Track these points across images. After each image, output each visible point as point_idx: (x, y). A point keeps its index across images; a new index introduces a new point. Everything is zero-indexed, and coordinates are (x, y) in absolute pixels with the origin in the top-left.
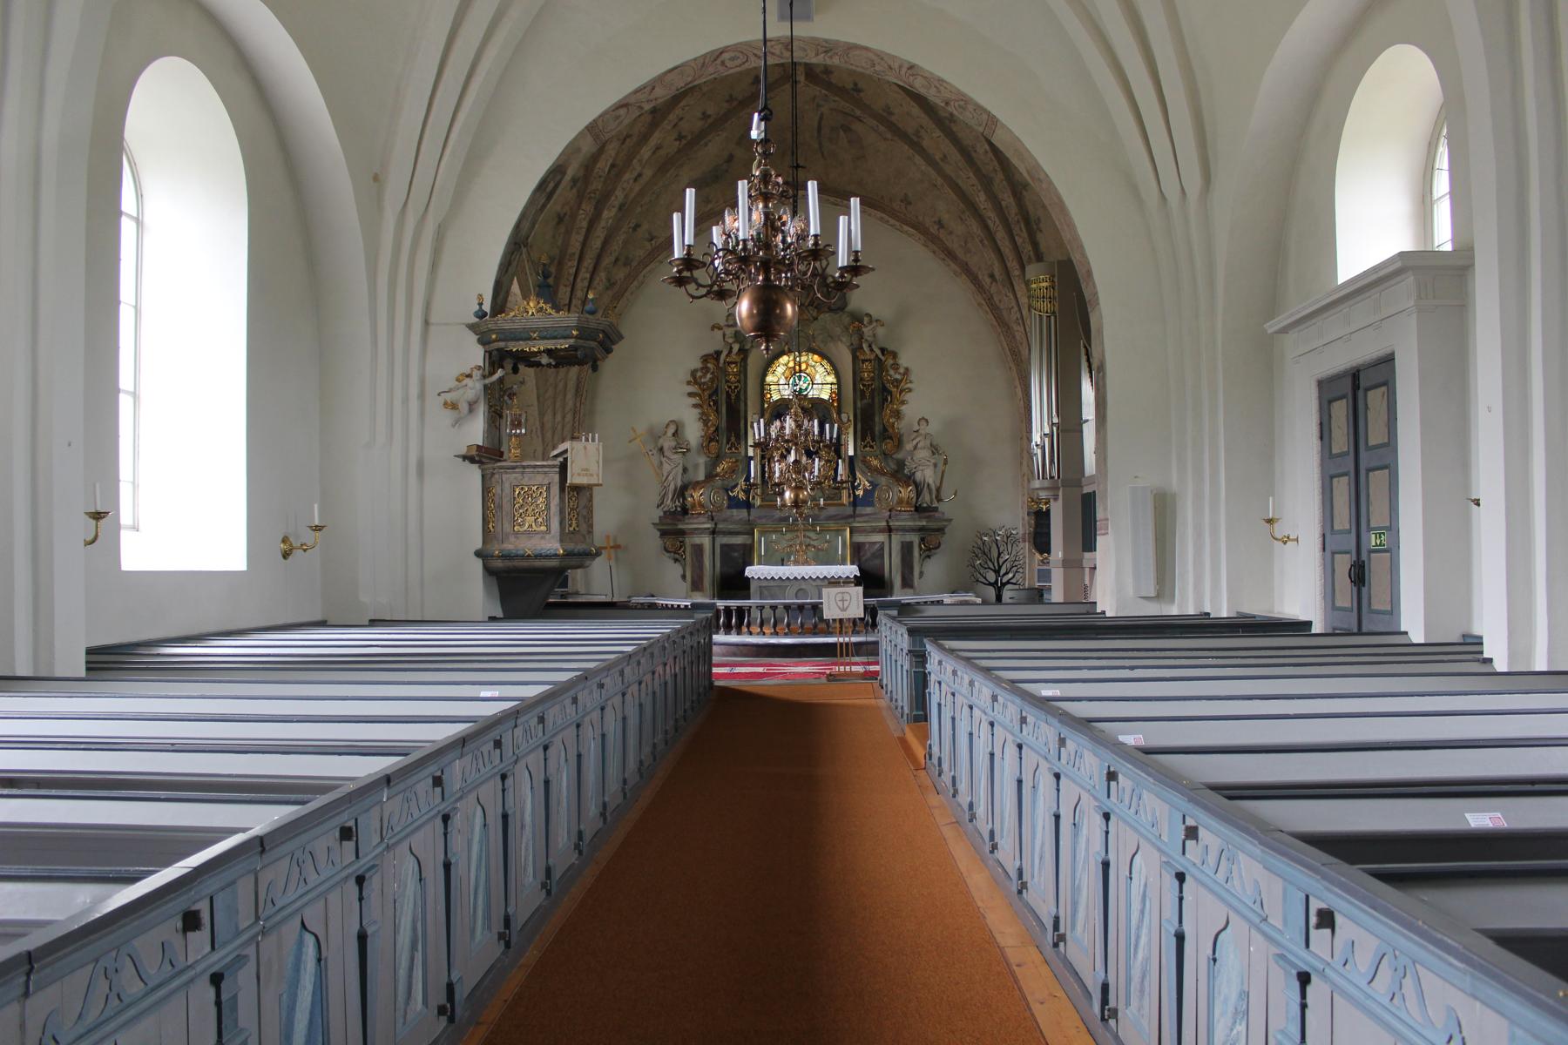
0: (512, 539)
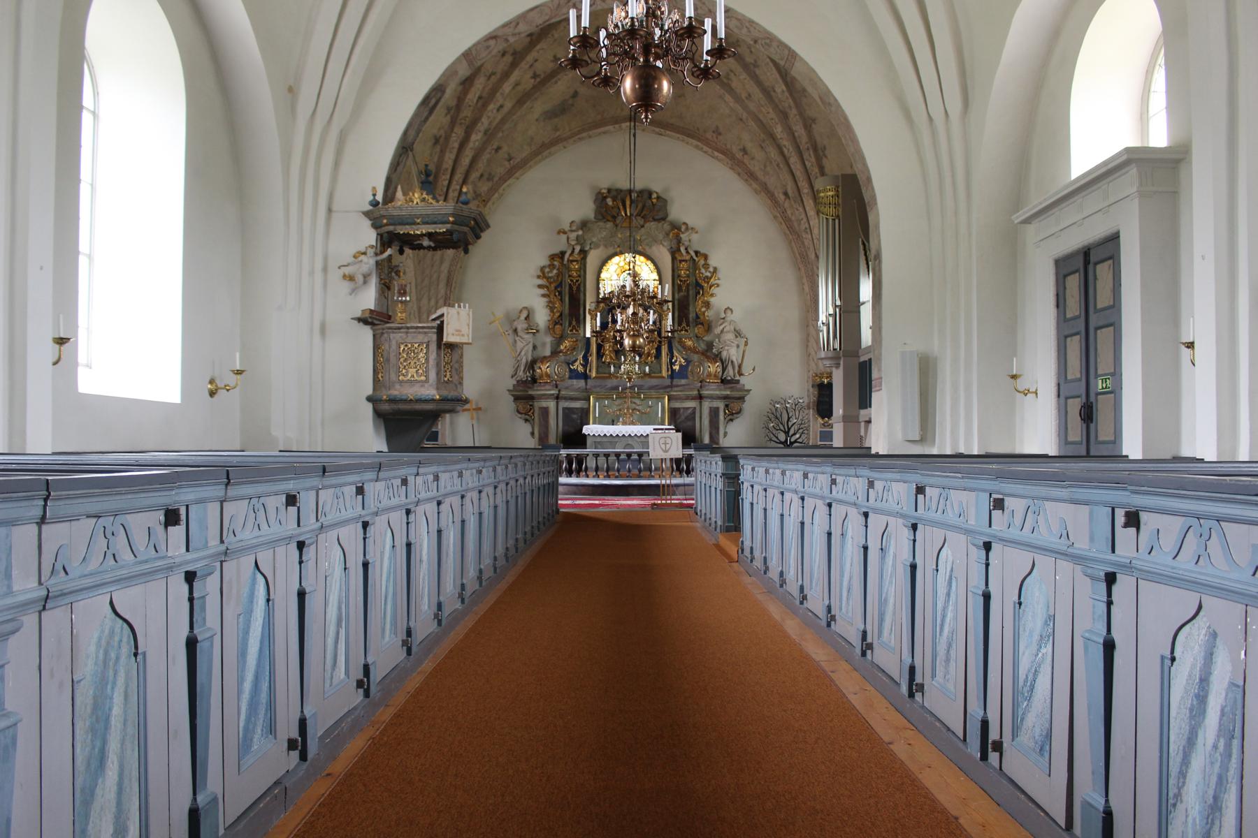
0: (397, 386)
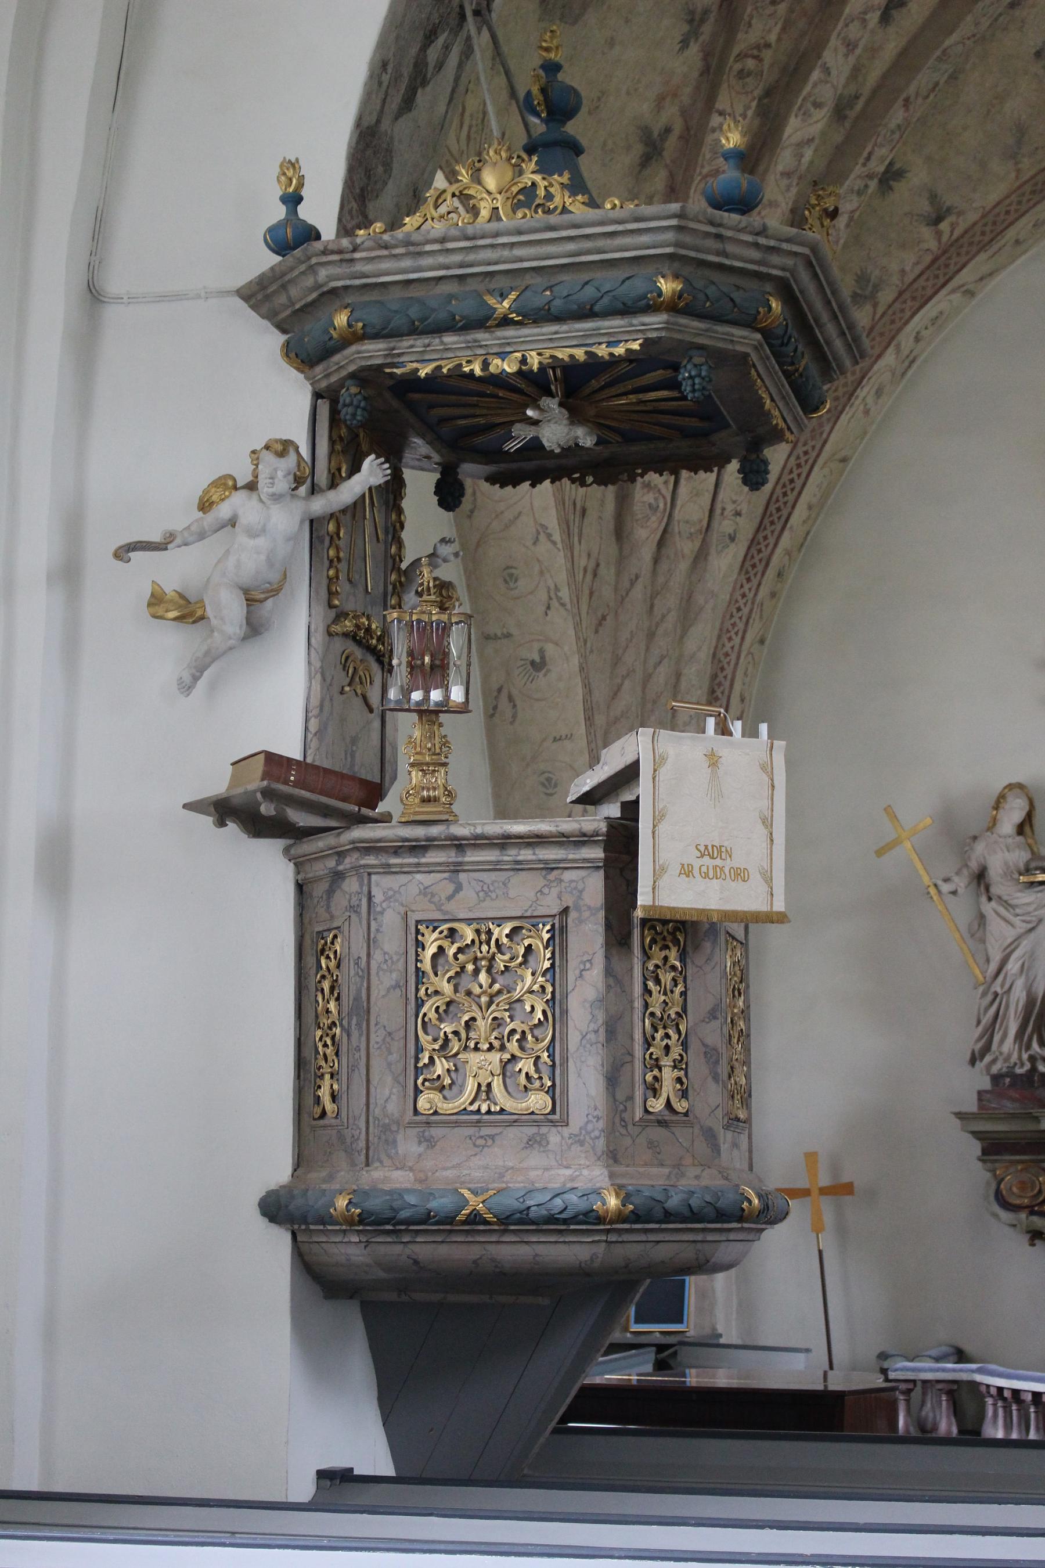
0: (408, 1145)
